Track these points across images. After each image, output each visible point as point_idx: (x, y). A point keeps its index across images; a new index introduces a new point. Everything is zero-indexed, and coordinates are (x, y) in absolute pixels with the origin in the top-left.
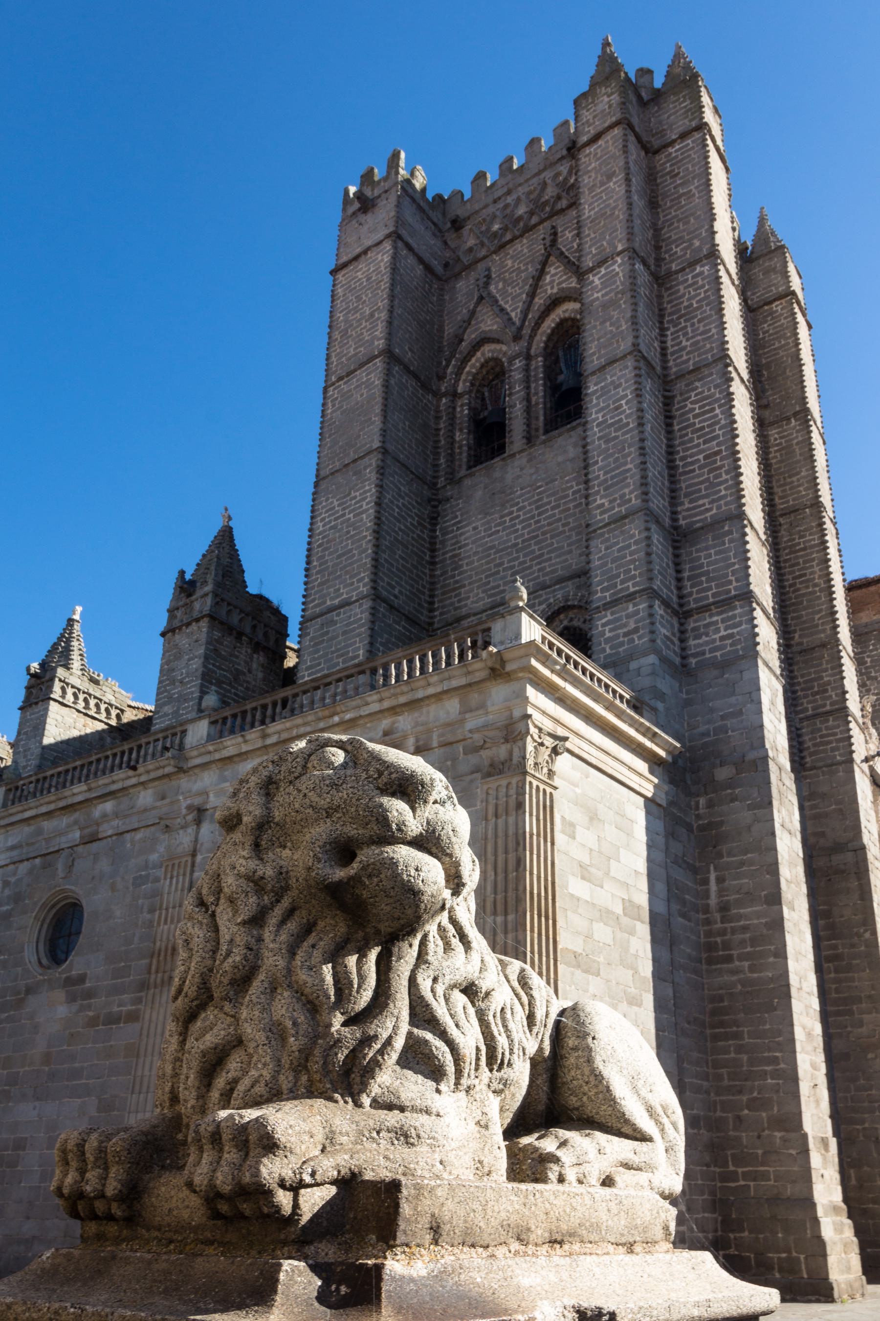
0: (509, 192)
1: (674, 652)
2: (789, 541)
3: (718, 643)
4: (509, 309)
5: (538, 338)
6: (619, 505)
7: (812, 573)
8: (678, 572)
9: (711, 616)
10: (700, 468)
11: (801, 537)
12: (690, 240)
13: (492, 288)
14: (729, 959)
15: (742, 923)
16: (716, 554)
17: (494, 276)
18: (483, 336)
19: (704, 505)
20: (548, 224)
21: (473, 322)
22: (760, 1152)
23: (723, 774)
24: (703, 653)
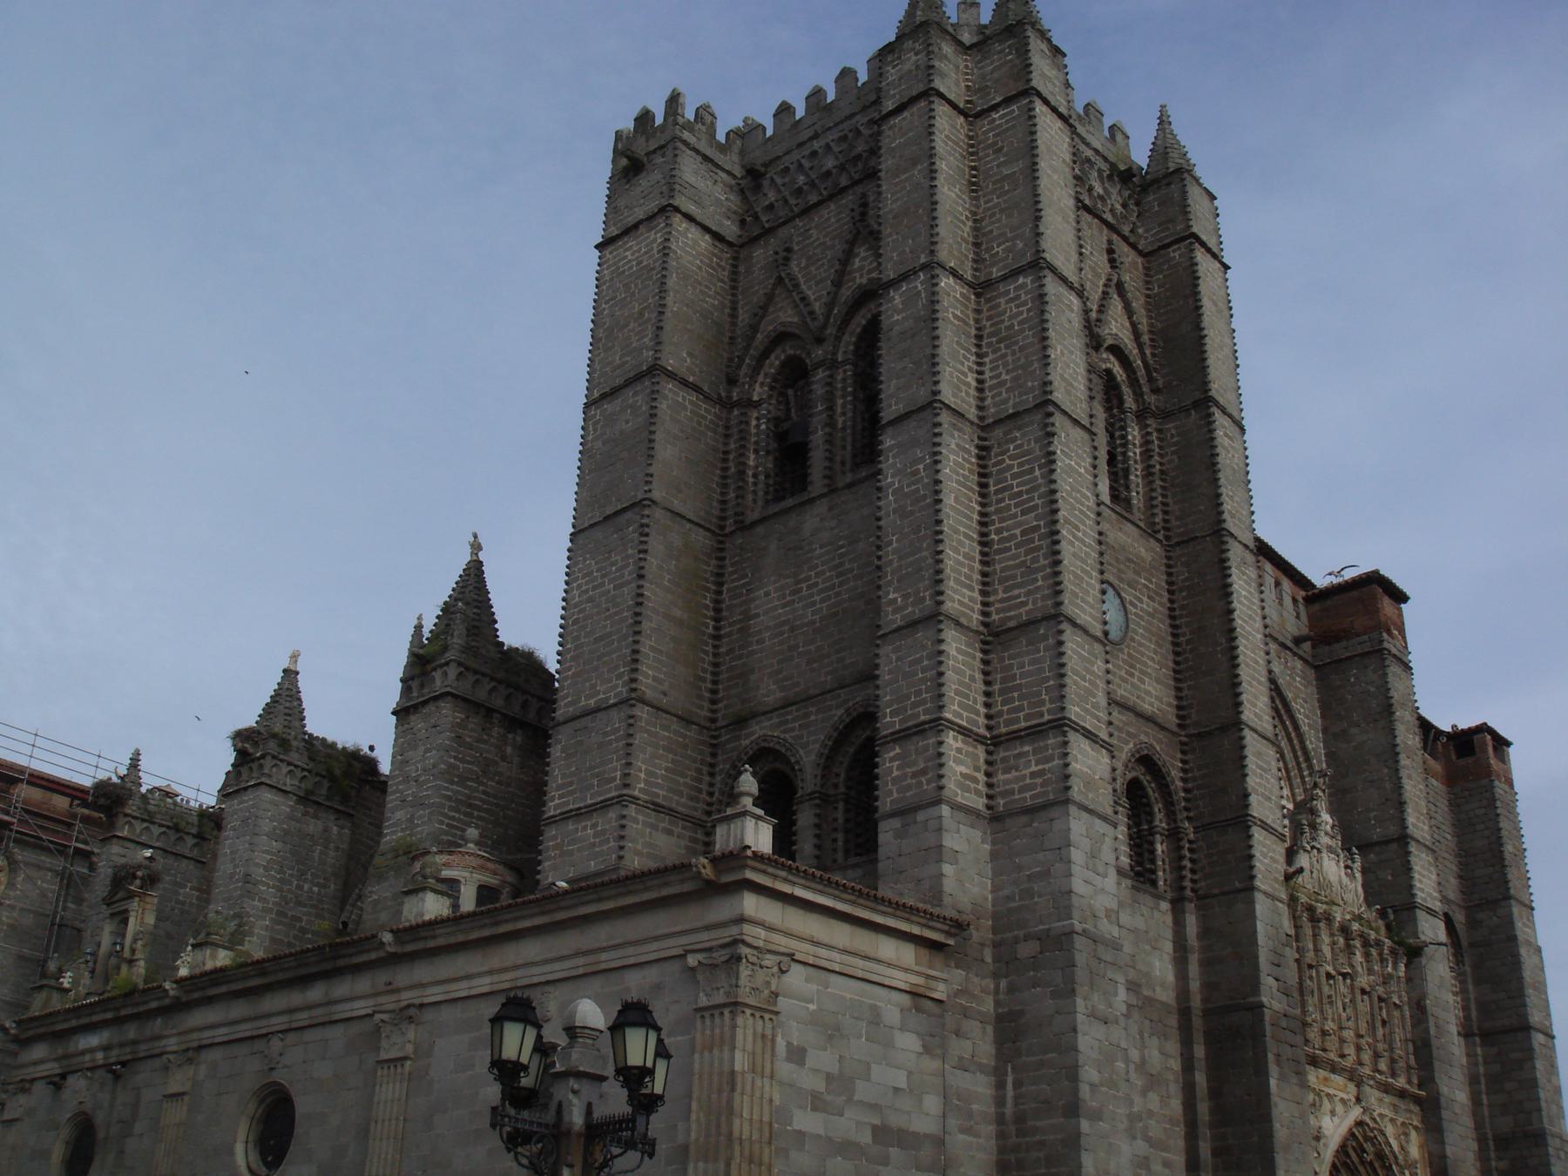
0: (816, 136)
1: (977, 792)
3: (1028, 781)
4: (812, 297)
5: (846, 337)
6: (914, 604)
9: (1022, 746)
10: (1018, 546)
12: (1013, 239)
13: (793, 264)
15: (1037, 1138)
16: (1031, 663)
17: (796, 248)
18: (782, 329)
19: (1018, 596)
20: (859, 189)
21: (771, 309)
24: (1012, 792)
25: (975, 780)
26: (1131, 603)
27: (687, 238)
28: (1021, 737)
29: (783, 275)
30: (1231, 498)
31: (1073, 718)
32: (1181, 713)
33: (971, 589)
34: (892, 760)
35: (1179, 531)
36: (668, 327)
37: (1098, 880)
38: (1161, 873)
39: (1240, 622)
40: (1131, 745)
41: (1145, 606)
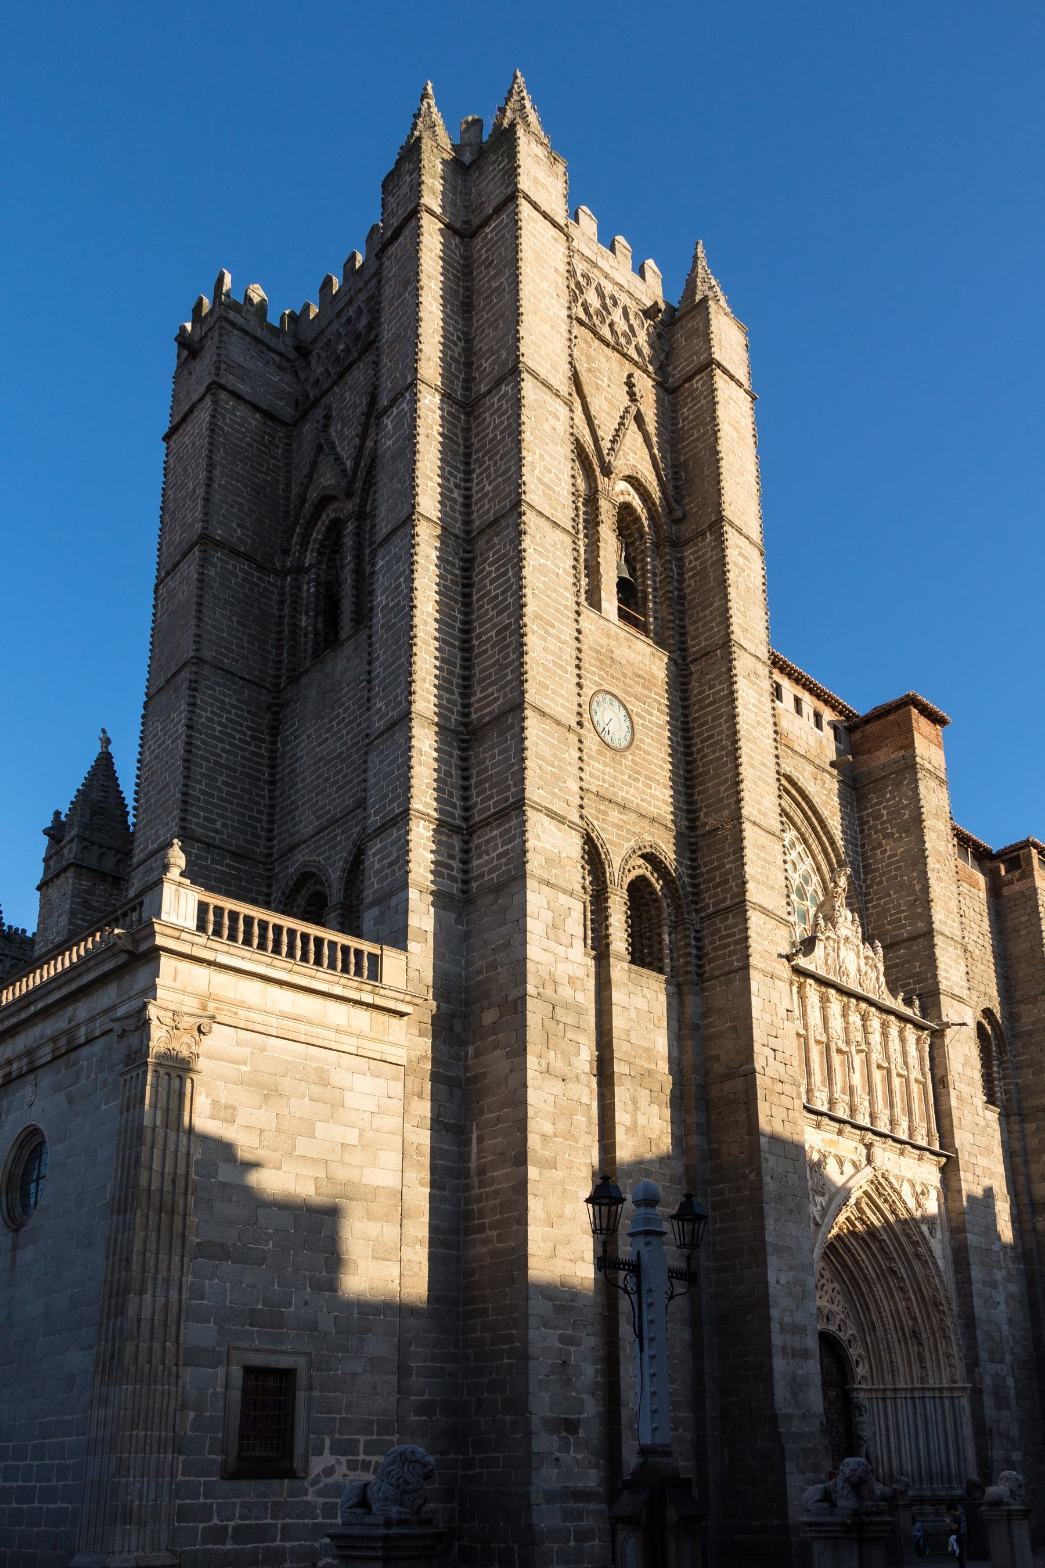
1: (451, 878)
2: (700, 693)
3: (496, 863)
6: (393, 709)
7: (720, 733)
8: (466, 778)
11: (711, 687)
14: (482, 1228)
15: (494, 1187)
18: (323, 493)
21: (315, 477)
22: (493, 1437)
23: (489, 1017)
25: (451, 868)
26: (638, 715)
27: (236, 415)
28: (490, 823)
29: (322, 441)
30: (744, 614)
31: (536, 799)
32: (690, 816)
33: (453, 693)
34: (374, 855)
35: (694, 650)
36: (217, 497)
37: (561, 950)
38: (667, 961)
39: (746, 727)
40: (632, 843)
41: (654, 719)
